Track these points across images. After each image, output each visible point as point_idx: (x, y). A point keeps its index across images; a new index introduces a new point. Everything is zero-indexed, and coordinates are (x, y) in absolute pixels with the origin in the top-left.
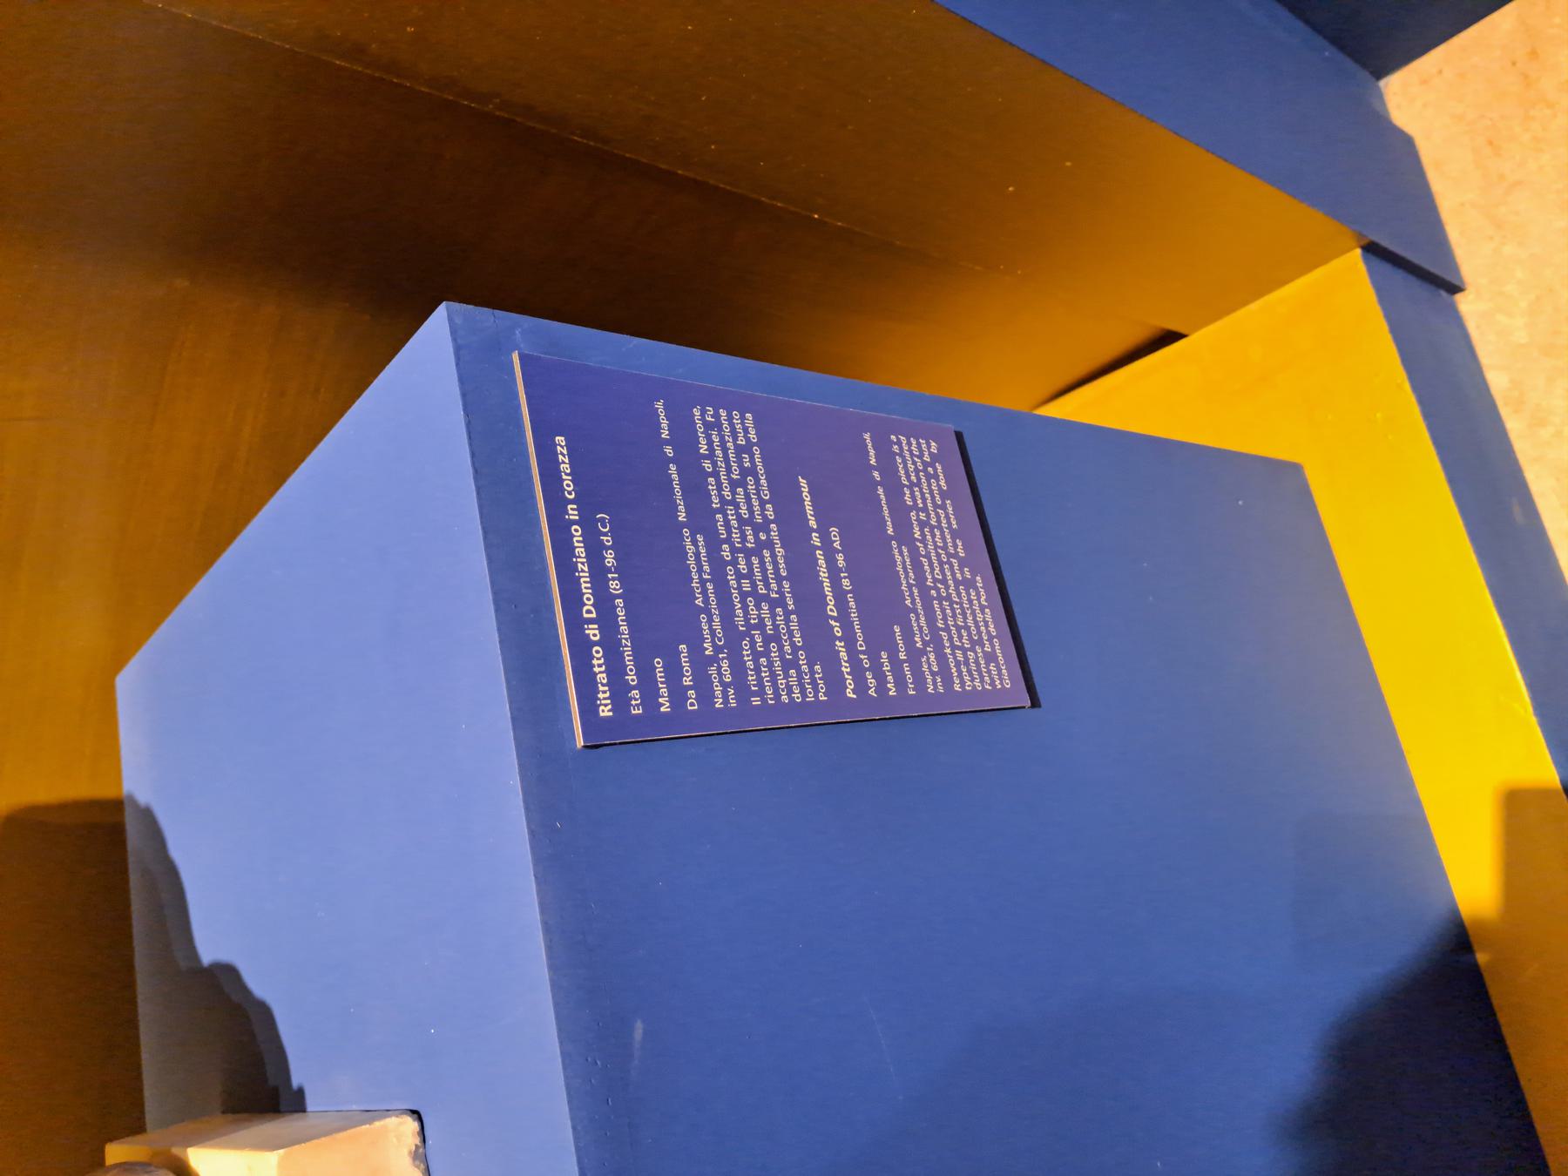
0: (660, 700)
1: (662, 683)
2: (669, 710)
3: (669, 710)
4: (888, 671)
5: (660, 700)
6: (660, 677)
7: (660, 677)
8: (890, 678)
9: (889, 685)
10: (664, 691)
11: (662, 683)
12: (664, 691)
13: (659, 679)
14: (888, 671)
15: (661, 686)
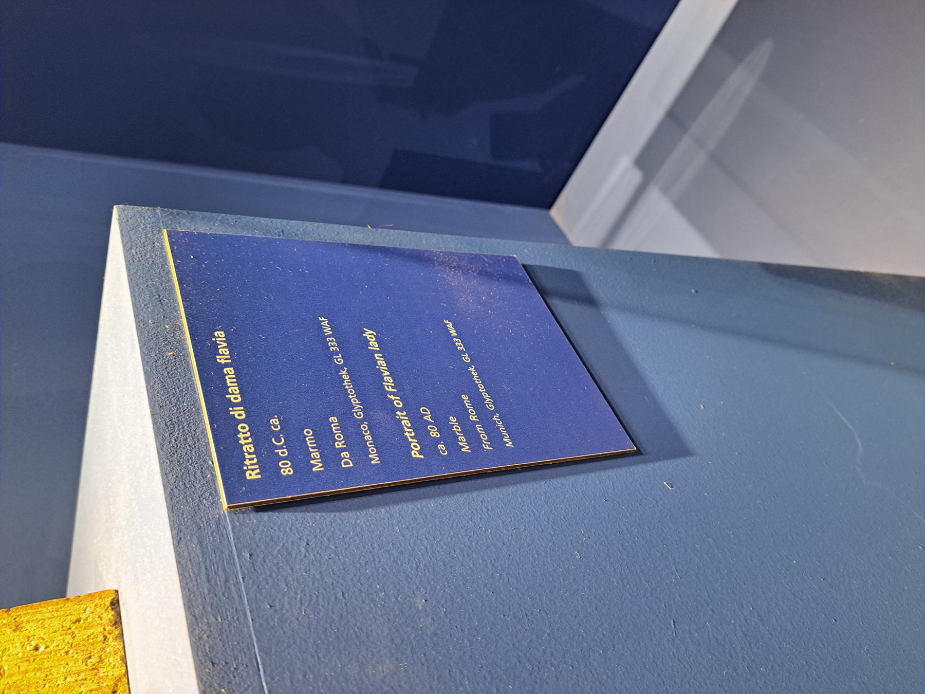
0: (312, 462)
3: (323, 469)
5: (312, 462)
6: (311, 443)
7: (311, 443)
10: (315, 454)
11: (313, 448)
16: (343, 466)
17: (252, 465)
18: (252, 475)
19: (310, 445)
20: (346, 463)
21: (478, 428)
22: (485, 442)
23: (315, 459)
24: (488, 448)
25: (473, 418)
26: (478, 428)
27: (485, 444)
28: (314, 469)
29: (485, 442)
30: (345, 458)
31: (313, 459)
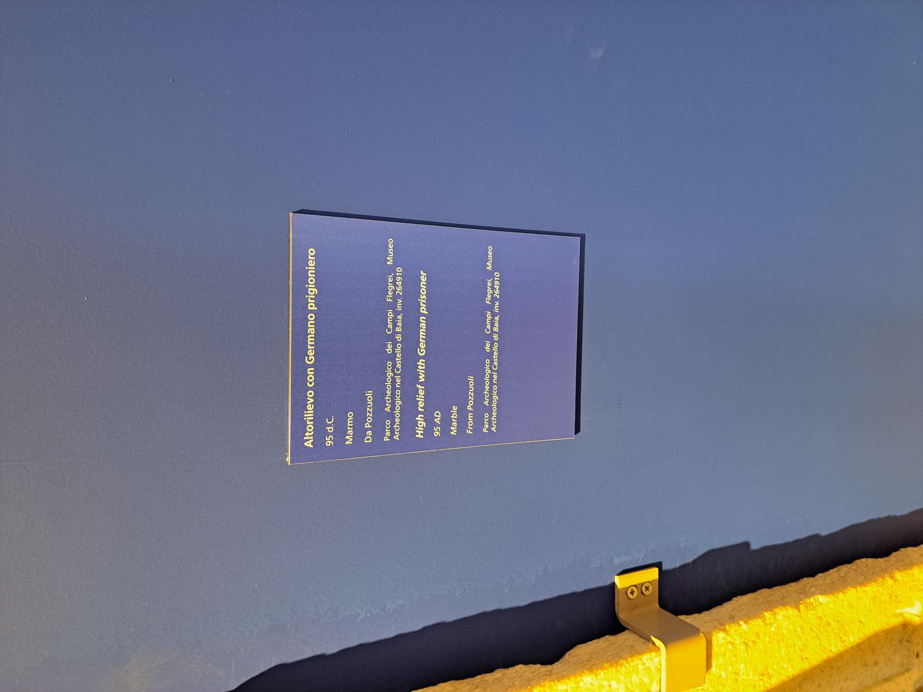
0: (347, 437)
1: (350, 427)
2: (352, 443)
3: (352, 443)
4: (454, 419)
5: (347, 437)
6: (350, 423)
7: (350, 423)
8: (455, 424)
9: (452, 428)
10: (350, 432)
11: (350, 427)
12: (350, 432)
13: (349, 425)
14: (454, 419)
15: (349, 428)
16: (366, 441)
17: (309, 436)
18: (309, 444)
19: (349, 425)
20: (368, 439)
21: (470, 416)
22: (469, 428)
23: (350, 435)
24: (470, 432)
25: (469, 408)
26: (470, 416)
27: (469, 429)
28: (347, 443)
29: (469, 428)
30: (368, 435)
31: (348, 435)
